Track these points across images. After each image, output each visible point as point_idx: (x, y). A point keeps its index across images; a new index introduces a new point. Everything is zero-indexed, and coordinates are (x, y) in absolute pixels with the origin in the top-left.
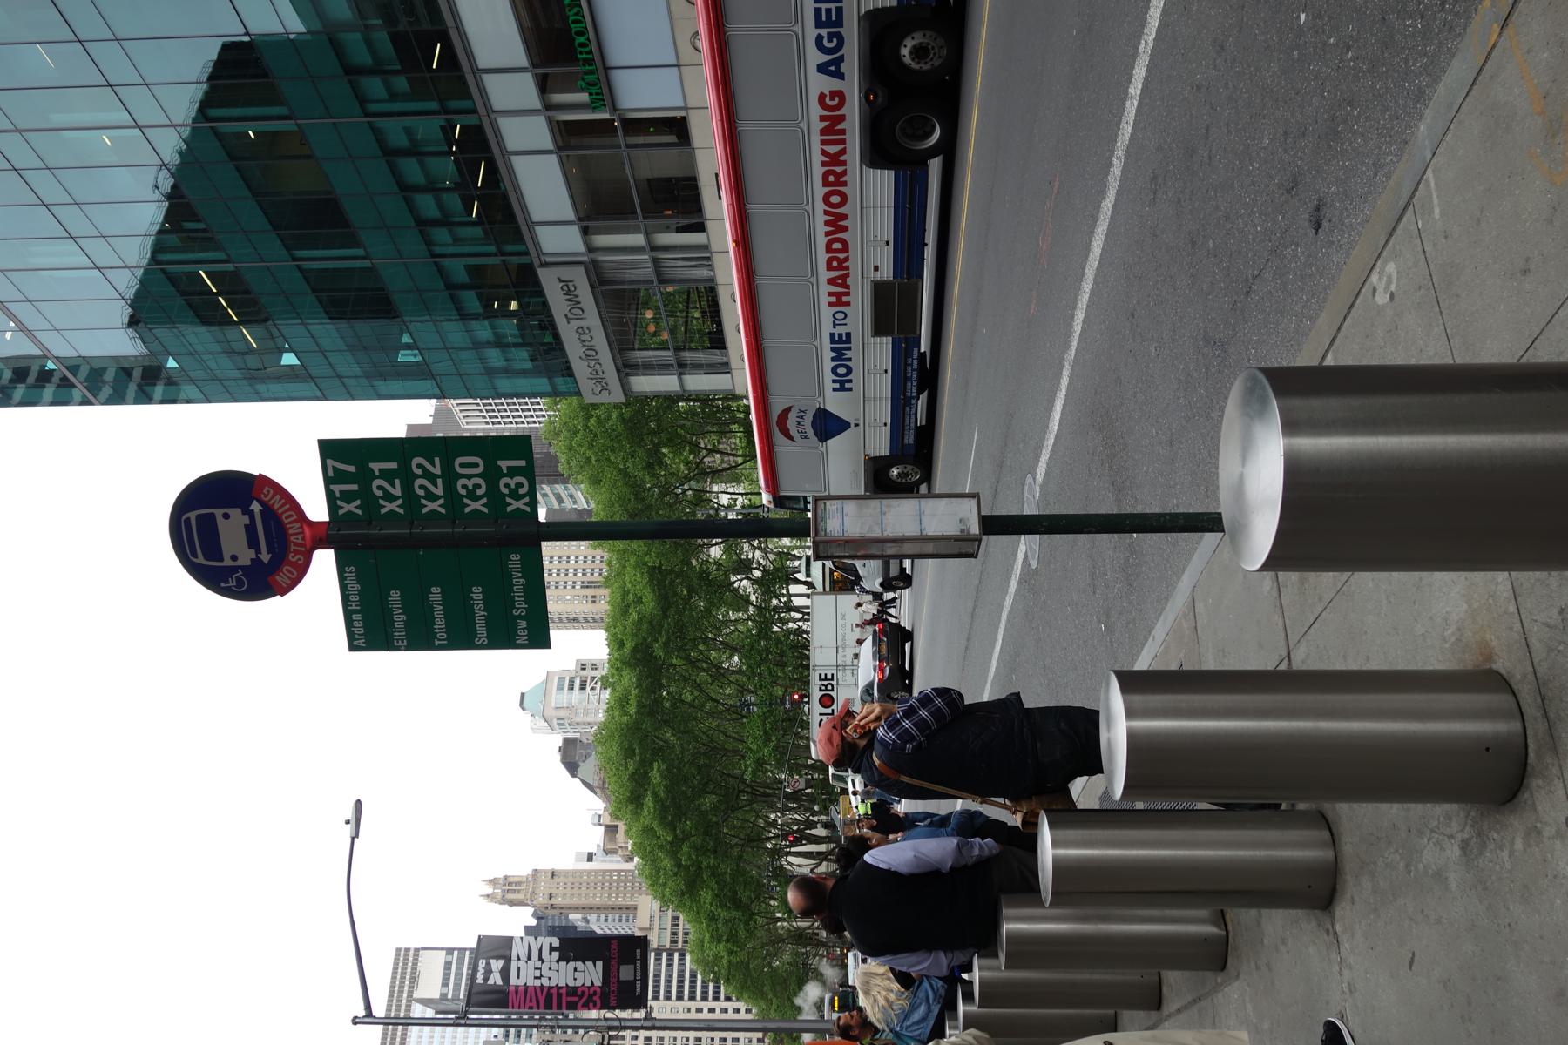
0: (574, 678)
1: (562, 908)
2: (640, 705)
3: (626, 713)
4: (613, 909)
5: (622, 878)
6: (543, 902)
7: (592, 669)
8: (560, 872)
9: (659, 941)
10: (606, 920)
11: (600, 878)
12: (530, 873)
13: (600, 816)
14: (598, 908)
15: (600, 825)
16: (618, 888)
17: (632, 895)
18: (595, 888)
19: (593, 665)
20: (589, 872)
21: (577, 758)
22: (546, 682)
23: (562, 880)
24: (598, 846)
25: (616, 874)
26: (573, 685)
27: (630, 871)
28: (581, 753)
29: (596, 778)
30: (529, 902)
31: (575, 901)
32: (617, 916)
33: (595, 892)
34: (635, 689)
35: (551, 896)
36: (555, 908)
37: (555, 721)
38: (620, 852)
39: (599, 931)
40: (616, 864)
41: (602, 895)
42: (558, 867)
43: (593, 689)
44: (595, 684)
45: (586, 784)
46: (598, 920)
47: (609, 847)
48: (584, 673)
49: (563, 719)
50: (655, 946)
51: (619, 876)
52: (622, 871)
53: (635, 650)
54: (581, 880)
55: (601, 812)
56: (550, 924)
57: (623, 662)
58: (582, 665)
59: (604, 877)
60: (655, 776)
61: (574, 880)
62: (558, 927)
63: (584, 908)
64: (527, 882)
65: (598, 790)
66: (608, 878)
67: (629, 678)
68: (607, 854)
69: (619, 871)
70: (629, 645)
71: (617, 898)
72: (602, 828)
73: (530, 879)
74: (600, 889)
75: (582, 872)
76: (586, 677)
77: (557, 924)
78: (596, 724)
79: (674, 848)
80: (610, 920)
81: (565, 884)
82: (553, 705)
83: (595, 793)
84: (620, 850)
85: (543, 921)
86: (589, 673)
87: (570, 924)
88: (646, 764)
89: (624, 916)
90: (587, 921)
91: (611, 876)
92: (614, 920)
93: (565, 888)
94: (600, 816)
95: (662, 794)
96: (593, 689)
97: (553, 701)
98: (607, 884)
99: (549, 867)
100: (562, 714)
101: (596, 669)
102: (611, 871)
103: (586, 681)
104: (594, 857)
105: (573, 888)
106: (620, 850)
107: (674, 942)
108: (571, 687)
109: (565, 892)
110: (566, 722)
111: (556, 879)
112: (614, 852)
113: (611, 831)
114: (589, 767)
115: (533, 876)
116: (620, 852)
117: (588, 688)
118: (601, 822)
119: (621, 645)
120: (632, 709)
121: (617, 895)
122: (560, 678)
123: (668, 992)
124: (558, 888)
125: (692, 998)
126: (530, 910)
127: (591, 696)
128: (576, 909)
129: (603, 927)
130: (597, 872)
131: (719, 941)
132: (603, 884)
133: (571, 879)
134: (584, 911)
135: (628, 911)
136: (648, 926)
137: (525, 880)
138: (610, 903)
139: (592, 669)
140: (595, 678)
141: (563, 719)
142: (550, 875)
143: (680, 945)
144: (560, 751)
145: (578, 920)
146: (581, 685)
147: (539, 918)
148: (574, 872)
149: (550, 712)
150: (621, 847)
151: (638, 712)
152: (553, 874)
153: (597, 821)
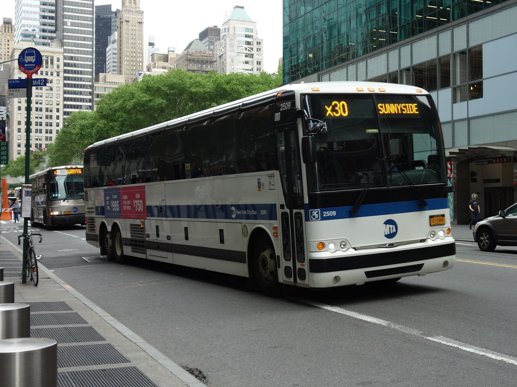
0: (252, 38)
2: (195, 93)
4: (120, 58)
5: (137, 63)
6: (124, 17)
7: (257, 49)
8: (142, 27)
9: (99, 87)
10: (114, 54)
11: (138, 51)
12: (141, 9)
14: (120, 49)
15: (169, 52)
16: (132, 61)
17: (128, 70)
18: (132, 48)
19: (260, 49)
20: (141, 44)
22: (250, 22)
23: (137, 28)
24: (158, 50)
25: (141, 60)
26: (248, 37)
28: (213, 39)
29: (193, 51)
30: (124, 8)
31: (124, 36)
32: (116, 60)
33: (130, 47)
34: (204, 91)
36: (121, 24)
37: (227, 27)
39: (108, 49)
40: (147, 61)
41: (128, 51)
42: (145, 25)
43: (246, 49)
44: (249, 50)
45: (190, 44)
46: (114, 49)
47: (155, 56)
48: (255, 43)
49: (228, 31)
50: (95, 85)
51: (140, 62)
52: (143, 64)
53: (225, 90)
54: (137, 39)
55: (175, 52)
56: (112, 20)
57: (218, 83)
58: (260, 43)
59: (139, 53)
61: (137, 35)
63: (120, 41)
64: (136, 8)
65: (186, 52)
66: (138, 55)
67: (210, 86)
68: (151, 55)
69: (142, 62)
70: (227, 87)
71: (126, 60)
72: (166, 53)
73: (138, 9)
75: (142, 39)
76: (252, 45)
77: (112, 24)
78: (225, 50)
80: (114, 56)
81: (135, 30)
82: (236, 26)
83: (185, 50)
84: (153, 63)
85: (114, 16)
86: (255, 47)
87: (112, 32)
88: (166, 96)
89: (116, 64)
90: (113, 43)
91: (139, 57)
93: (132, 30)
94: (173, 51)
96: (246, 49)
97: (239, 26)
99: (145, 20)
100: (231, 31)
101: (257, 51)
102: (142, 57)
103: (250, 45)
104: (152, 47)
105: (132, 34)
106: (153, 63)
107: (98, 96)
108: (247, 36)
109: (130, 30)
110: (227, 33)
111: (137, 25)
112: (153, 60)
113: (165, 58)
114: (203, 47)
115: (140, 11)
117: (247, 46)
118: (170, 52)
119: (228, 83)
121: (128, 61)
122: (252, 29)
124: (132, 25)
125: (65, 106)
126: (120, 8)
127: (241, 48)
128: (120, 36)
129: (110, 52)
130: (142, 49)
131: (81, 129)
132: (135, 52)
133: (137, 33)
134: (119, 41)
135: (119, 67)
136: (107, 81)
137: (137, 6)
138: (123, 56)
139: (257, 49)
140: (252, 50)
141: (228, 31)
142: (140, 21)
143: (96, 99)
144: (214, 26)
145: (114, 37)
146: (248, 42)
147: (116, 13)
149: (232, 24)
150: (155, 64)
152: (140, 23)
153: (171, 49)
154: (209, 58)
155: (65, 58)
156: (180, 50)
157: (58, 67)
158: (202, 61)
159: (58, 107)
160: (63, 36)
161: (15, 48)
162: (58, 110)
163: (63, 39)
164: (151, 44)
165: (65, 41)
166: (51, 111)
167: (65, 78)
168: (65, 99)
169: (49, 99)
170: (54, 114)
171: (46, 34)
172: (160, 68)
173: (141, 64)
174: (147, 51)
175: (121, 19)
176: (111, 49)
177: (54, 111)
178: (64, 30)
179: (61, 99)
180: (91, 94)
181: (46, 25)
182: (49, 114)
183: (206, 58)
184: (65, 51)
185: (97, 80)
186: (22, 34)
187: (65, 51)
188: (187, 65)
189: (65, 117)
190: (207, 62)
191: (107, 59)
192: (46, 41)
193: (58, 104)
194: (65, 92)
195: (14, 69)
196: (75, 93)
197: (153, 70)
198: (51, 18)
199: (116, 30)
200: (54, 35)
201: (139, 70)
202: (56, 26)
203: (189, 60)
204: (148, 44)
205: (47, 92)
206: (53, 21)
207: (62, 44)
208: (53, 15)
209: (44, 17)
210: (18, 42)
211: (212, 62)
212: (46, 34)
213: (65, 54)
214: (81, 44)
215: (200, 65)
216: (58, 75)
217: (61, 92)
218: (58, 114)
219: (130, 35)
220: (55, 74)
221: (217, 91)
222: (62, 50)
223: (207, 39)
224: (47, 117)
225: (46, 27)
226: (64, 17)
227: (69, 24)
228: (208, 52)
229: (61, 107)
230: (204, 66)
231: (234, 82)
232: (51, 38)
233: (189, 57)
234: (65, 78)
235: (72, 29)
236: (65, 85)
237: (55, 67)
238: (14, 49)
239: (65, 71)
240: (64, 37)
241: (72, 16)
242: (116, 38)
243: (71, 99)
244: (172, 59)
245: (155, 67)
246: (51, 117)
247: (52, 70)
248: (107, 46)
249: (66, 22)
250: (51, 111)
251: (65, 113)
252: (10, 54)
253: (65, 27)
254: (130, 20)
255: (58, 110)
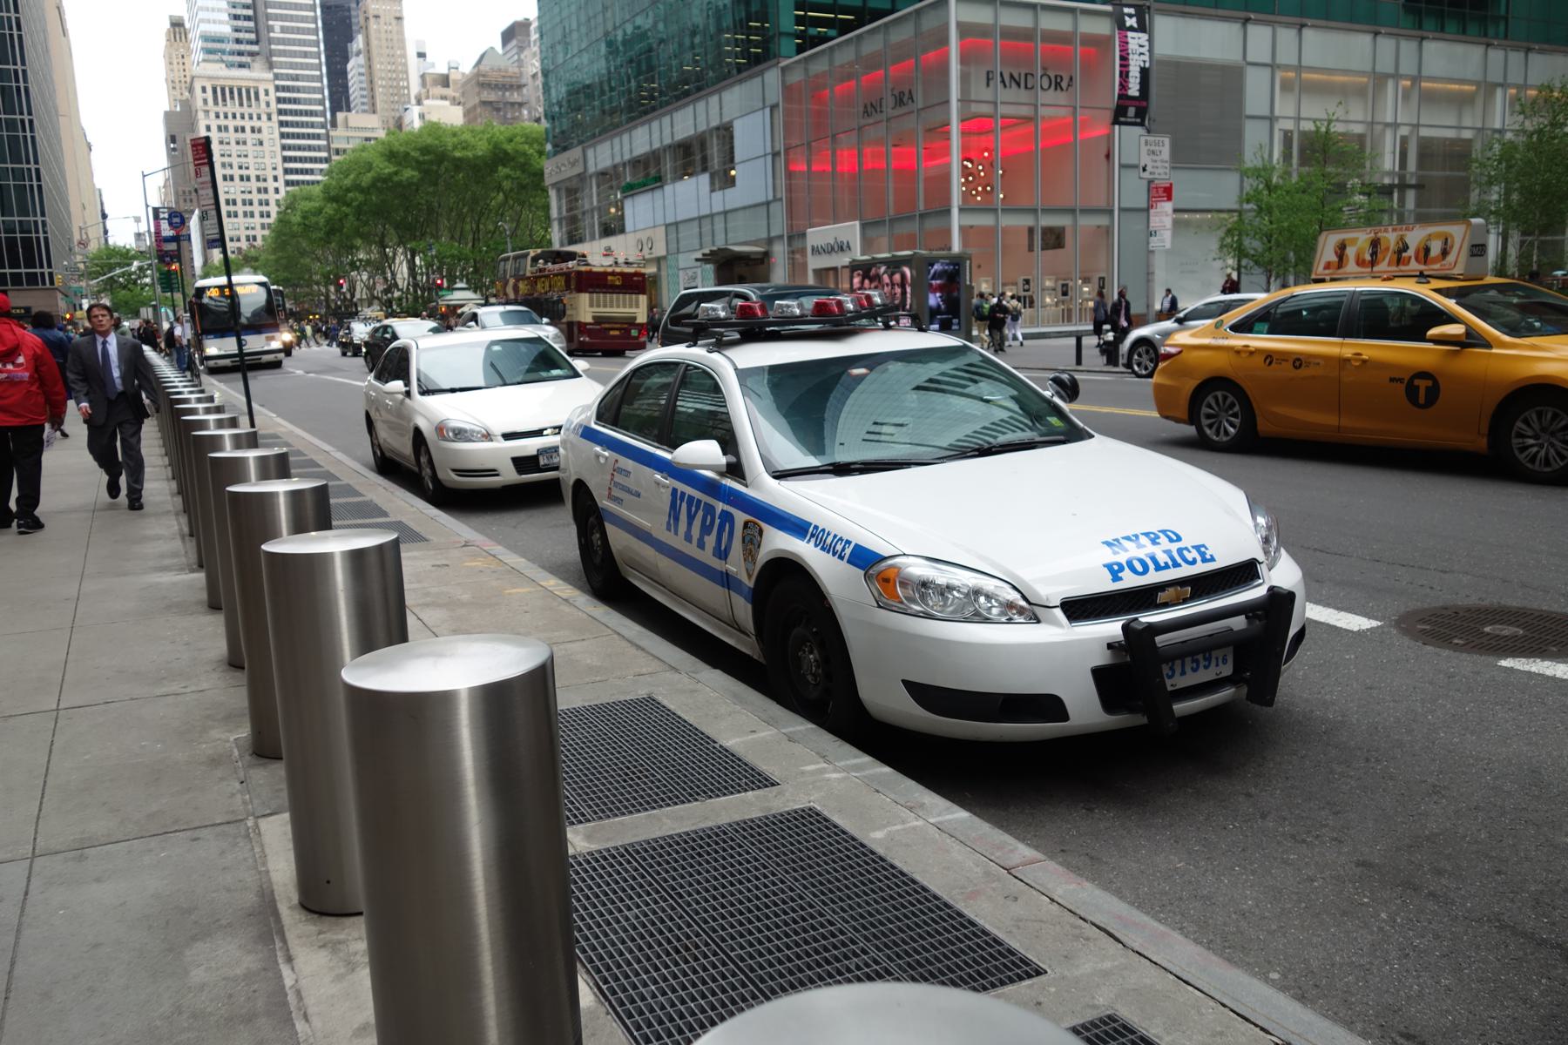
1: (367, 28)
3: (455, 148)
9: (337, 137)
10: (360, 74)
13: (457, 68)
14: (370, 67)
15: (449, 69)
17: (386, 102)
20: (404, 56)
21: (519, 38)
23: (393, 27)
24: (433, 65)
25: (405, 84)
27: (409, 98)
31: (374, 43)
32: (364, 85)
35: (377, 17)
38: (424, 91)
39: (349, 66)
42: (406, 23)
46: (359, 66)
50: (331, 133)
51: (404, 88)
53: (506, 153)
55: (461, 69)
59: (401, 72)
60: (409, 174)
62: (351, 22)
65: (476, 70)
70: (509, 148)
72: (444, 71)
74: (389, 68)
75: (403, 48)
79: (357, 187)
90: (358, 54)
91: (402, 79)
92: (361, 82)
94: (457, 68)
95: (396, 179)
98: (394, 76)
99: (406, 14)
102: (407, 79)
107: (337, 152)
111: (394, 22)
112: (424, 84)
116: (424, 91)
119: (511, 140)
120: (458, 154)
121: (383, 87)
123: (290, 148)
128: (367, 43)
130: (405, 65)
132: (394, 71)
133: (395, 38)
136: (350, 125)
142: (398, 15)
143: (335, 158)
148: (402, 41)
151: (455, 159)
152: (399, 19)
153: (452, 65)
154: (514, 80)
155: (277, 89)
156: (467, 68)
157: (268, 104)
158: (504, 86)
159: (275, 173)
160: (271, 50)
161: (194, 74)
162: (276, 179)
163: (271, 56)
164: (421, 55)
165: (274, 59)
166: (265, 180)
167: (282, 124)
168: (286, 159)
169: (259, 160)
170: (271, 185)
171: (242, 47)
172: (437, 98)
173: (406, 91)
174: (414, 68)
175: (365, 12)
176: (354, 66)
177: (270, 179)
178: (271, 40)
179: (279, 160)
180: (328, 149)
181: (240, 31)
182: (262, 185)
183: (509, 80)
184: (277, 77)
185: (334, 124)
186: (202, 49)
187: (277, 77)
188: (478, 94)
189: (289, 189)
190: (511, 86)
191: (350, 84)
192: (244, 59)
193: (275, 169)
194: (284, 148)
195: (196, 111)
196: (299, 148)
197: (426, 102)
198: (247, 18)
199: (359, 32)
200: (255, 48)
201: (404, 103)
202: (257, 32)
203: (482, 85)
204: (415, 55)
205: (255, 148)
206: (251, 24)
207: (271, 66)
208: (250, 12)
209: (236, 17)
210: (198, 64)
211: (520, 87)
212: (242, 47)
213: (277, 82)
214: (301, 64)
215: (500, 93)
216: (269, 119)
217: (278, 148)
218: (276, 185)
219: (384, 41)
220: (264, 117)
221: (495, 154)
222: (271, 76)
223: (514, 42)
224: (259, 191)
225: (241, 35)
226: (268, 17)
227: (277, 29)
228: (513, 70)
229: (280, 172)
230: (507, 94)
231: (518, 139)
232: (252, 54)
233: (481, 79)
234: (282, 124)
235: (283, 39)
236: (283, 136)
237: (263, 105)
238: (193, 78)
239: (280, 112)
240: (272, 53)
241: (281, 15)
242: (361, 46)
243: (295, 159)
244: (455, 82)
245: (428, 98)
246: (266, 191)
247: (258, 111)
248: (346, 60)
249: (272, 26)
250: (265, 180)
251: (288, 183)
252: (188, 85)
253: (272, 35)
254: (381, 13)
255: (276, 179)
